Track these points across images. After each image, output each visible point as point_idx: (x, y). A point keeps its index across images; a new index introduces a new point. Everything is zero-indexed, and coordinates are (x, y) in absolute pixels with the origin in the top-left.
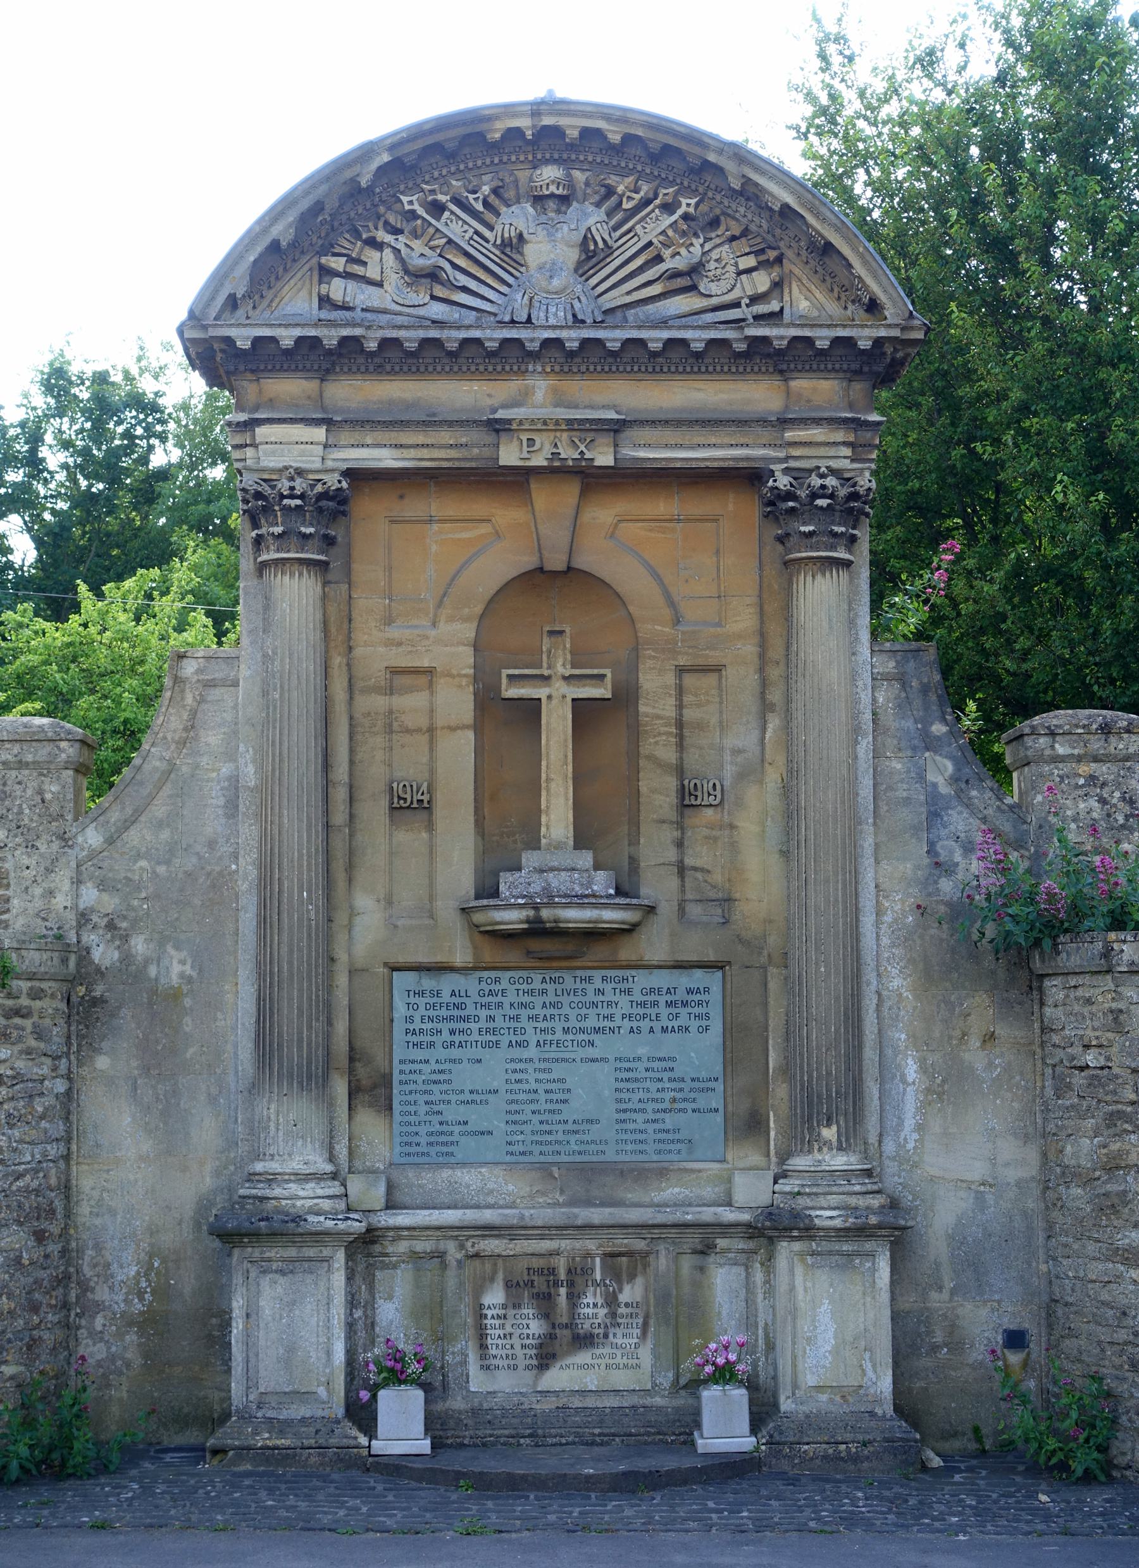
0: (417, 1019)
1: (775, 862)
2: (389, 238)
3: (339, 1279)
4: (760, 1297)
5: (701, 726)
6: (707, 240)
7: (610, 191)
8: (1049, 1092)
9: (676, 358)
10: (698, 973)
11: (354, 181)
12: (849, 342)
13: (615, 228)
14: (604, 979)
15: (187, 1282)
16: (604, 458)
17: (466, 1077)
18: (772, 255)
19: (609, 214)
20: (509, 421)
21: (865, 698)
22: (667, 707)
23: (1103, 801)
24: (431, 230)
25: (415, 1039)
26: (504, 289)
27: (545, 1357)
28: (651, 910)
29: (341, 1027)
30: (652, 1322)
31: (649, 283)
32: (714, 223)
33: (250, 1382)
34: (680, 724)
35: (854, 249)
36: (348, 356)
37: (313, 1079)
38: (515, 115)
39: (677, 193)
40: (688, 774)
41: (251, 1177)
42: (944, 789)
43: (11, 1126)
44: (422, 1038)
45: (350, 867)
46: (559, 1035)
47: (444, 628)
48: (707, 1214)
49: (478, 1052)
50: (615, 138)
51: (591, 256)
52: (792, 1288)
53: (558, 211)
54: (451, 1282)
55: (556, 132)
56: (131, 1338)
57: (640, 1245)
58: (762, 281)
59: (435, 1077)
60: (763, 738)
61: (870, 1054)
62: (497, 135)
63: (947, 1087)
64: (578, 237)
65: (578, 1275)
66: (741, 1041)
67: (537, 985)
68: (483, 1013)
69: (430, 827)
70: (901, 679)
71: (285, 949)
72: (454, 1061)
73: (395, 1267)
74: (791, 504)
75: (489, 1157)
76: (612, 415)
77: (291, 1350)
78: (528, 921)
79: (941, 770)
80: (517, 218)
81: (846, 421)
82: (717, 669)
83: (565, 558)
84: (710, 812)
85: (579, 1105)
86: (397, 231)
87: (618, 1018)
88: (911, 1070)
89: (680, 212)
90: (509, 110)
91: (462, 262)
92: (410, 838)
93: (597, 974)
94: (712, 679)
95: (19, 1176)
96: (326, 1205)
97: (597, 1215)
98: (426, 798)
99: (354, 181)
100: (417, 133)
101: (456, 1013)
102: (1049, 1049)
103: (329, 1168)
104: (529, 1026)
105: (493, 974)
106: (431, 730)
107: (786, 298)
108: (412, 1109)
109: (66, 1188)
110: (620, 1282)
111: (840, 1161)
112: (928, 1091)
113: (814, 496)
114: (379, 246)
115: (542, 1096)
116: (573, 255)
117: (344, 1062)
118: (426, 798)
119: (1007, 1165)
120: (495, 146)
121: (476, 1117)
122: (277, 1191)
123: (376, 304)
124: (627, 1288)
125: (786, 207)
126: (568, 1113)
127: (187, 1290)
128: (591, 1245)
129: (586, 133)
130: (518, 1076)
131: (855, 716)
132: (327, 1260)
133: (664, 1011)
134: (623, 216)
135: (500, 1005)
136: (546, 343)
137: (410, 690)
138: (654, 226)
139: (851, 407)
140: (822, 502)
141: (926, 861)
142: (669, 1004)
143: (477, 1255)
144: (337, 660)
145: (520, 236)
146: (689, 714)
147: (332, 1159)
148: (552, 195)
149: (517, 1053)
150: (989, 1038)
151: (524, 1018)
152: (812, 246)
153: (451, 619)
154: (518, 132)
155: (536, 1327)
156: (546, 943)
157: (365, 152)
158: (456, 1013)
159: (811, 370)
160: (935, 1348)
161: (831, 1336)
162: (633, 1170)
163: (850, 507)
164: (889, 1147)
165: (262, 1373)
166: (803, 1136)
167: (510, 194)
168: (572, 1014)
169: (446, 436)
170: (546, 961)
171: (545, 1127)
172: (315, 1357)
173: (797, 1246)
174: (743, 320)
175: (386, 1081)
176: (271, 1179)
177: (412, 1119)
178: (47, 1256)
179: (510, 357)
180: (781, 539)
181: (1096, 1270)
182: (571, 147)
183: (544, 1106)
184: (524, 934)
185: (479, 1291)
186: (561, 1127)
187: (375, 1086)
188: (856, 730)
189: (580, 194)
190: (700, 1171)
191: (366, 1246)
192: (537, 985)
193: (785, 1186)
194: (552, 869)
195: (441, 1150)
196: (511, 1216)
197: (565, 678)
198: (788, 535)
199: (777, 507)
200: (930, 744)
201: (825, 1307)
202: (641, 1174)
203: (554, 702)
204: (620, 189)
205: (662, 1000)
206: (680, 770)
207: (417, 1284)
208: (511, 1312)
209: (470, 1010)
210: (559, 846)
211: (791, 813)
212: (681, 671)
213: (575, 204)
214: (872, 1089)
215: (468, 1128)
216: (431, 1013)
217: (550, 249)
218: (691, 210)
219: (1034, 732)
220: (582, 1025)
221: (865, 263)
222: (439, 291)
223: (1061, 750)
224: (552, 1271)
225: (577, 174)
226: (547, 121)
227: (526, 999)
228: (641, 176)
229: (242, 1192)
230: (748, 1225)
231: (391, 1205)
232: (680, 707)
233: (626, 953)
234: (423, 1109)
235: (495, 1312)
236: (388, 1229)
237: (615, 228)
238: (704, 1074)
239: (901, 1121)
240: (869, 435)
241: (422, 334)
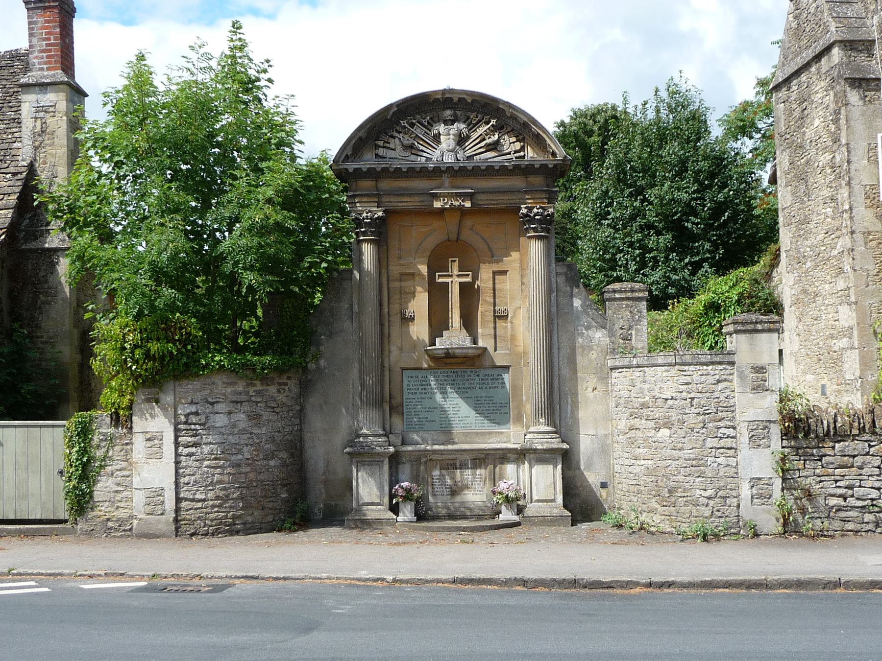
2: (397, 135)
3: (386, 467)
7: (469, 118)
16: (468, 204)
18: (521, 137)
19: (468, 125)
21: (554, 280)
23: (631, 312)
32: (502, 128)
34: (494, 290)
36: (385, 173)
50: (469, 101)
51: (461, 140)
55: (451, 99)
58: (518, 146)
67: (449, 374)
75: (435, 428)
86: (399, 132)
113: (535, 215)
114: (394, 137)
121: (430, 417)
123: (393, 156)
129: (460, 99)
132: (382, 462)
137: (407, 280)
138: (483, 129)
144: (384, 271)
157: (390, 106)
164: (563, 424)
169: (416, 198)
181: (627, 462)
182: (455, 103)
190: (502, 433)
192: (449, 374)
205: (489, 378)
207: (412, 470)
222: (414, 151)
223: (617, 296)
232: (494, 284)
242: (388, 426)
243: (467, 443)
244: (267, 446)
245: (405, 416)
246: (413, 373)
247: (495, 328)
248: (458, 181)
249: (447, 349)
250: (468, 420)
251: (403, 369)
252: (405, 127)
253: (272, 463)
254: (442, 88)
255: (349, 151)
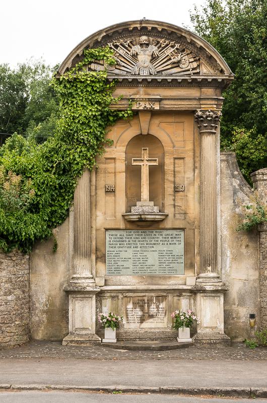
0: (112, 241)
1: (197, 204)
4: (193, 306)
5: (179, 172)
6: (182, 54)
7: (158, 42)
8: (261, 259)
9: (175, 84)
10: (179, 231)
11: (97, 40)
12: (216, 80)
13: (160, 51)
14: (156, 232)
15: (58, 302)
16: (157, 107)
17: (123, 255)
18: (197, 58)
19: (158, 48)
20: (134, 99)
22: (171, 168)
24: (115, 52)
25: (111, 246)
26: (133, 66)
27: (142, 320)
28: (168, 215)
29: (94, 243)
30: (167, 312)
31: (168, 65)
32: (183, 51)
33: (73, 326)
34: (174, 172)
35: (218, 57)
37: (88, 255)
38: (136, 24)
39: (175, 43)
40: (176, 184)
41: (73, 278)
42: (237, 187)
43: (17, 266)
44: (112, 246)
45: (96, 205)
46: (145, 245)
47: (117, 148)
48: (181, 287)
49: (126, 249)
50: (160, 30)
51: (154, 58)
52: (201, 304)
53: (146, 47)
54: (120, 303)
55: (146, 28)
56: (44, 316)
57: (165, 294)
58: (195, 65)
59: (116, 255)
60: (194, 175)
61: (219, 250)
62: (131, 29)
63: (237, 257)
64: (151, 53)
65: (150, 301)
66: (188, 247)
67: (140, 233)
68: (127, 240)
69: (115, 196)
70: (227, 161)
71: (81, 225)
72: (120, 251)
73: (107, 299)
74: (202, 119)
76: (159, 97)
77: (83, 318)
78: (138, 218)
79: (236, 183)
80: (136, 49)
81: (215, 99)
82: (183, 158)
83: (147, 131)
84: (181, 192)
85: (149, 262)
87: (159, 241)
88: (229, 254)
89: (175, 48)
90: (134, 22)
91: (123, 60)
92: (110, 198)
93: (154, 231)
94: (182, 161)
95: (19, 278)
96: (91, 284)
97: (154, 287)
98: (114, 189)
99: (97, 40)
100: (112, 28)
101: (121, 240)
102: (261, 248)
103: (91, 276)
104: (138, 243)
105: (130, 231)
106: (115, 173)
107: (201, 69)
108: (110, 262)
109: (29, 281)
110: (160, 303)
111: (212, 275)
112: (233, 258)
113: (207, 117)
115: (141, 260)
116: (150, 58)
117: (95, 252)
118: (114, 189)
119: (251, 276)
120: (131, 31)
121: (126, 264)
122: (79, 281)
124: (161, 304)
125: (201, 46)
126: (148, 263)
127: (58, 305)
128: (153, 294)
129: (153, 28)
130: (136, 255)
131: (216, 170)
133: (170, 239)
134: (162, 48)
135: (131, 238)
136: (143, 79)
138: (169, 51)
139: (216, 95)
140: (209, 119)
141: (233, 204)
142: (171, 238)
143: (126, 297)
145: (137, 53)
146: (177, 169)
147: (92, 274)
148: (145, 43)
149: (135, 249)
150: (247, 246)
151: (137, 241)
152: (207, 56)
153: (120, 146)
154: (136, 28)
155: (140, 313)
156: (143, 224)
157: (100, 32)
158: (121, 240)
159: (207, 86)
160: (233, 318)
161: (210, 315)
162: (162, 277)
163: (215, 120)
165: (76, 324)
166: (203, 268)
167: (134, 43)
168: (148, 240)
170: (142, 227)
171: (142, 267)
172: (89, 320)
173: (202, 294)
174: (191, 74)
175: (104, 256)
176: (78, 278)
177: (111, 265)
178: (25, 296)
179: (134, 83)
180: (199, 127)
182: (149, 31)
183: (141, 262)
184: (137, 221)
185: (126, 305)
186: (146, 267)
187: (102, 257)
188: (216, 174)
189: (151, 44)
190: (179, 277)
191: (100, 295)
193: (199, 280)
194: (144, 206)
195: (118, 271)
196: (134, 287)
197: (147, 160)
198: (201, 126)
199: (199, 121)
200: (234, 176)
201: (208, 308)
202: (164, 278)
203: (144, 166)
204: (161, 42)
206: (174, 183)
207: (112, 304)
208: (134, 310)
209: (124, 239)
210: (145, 201)
211: (201, 193)
212: (175, 159)
213: (150, 46)
214: (219, 258)
215: (124, 267)
216: (115, 240)
217: (144, 57)
218: (178, 47)
219: (259, 174)
220: (151, 243)
221: (220, 61)
224: (144, 300)
225: (150, 38)
226: (143, 25)
227: (137, 237)
228: (166, 39)
229: (71, 282)
230: (190, 290)
231: (106, 285)
232: (174, 167)
233: (161, 226)
234: (113, 262)
235: (130, 310)
236: (105, 290)
237: (160, 51)
238: (179, 254)
239: (226, 266)
240: (220, 102)
241: (113, 77)
242: (94, 272)
243: (152, 285)
244: (6, 286)
245: (107, 264)
246: (114, 232)
247: (174, 200)
248: (150, 91)
249: (140, 215)
250: (154, 268)
251: (107, 230)
252: (111, 48)
253: (9, 298)
254: (139, 19)
255: (69, 65)
